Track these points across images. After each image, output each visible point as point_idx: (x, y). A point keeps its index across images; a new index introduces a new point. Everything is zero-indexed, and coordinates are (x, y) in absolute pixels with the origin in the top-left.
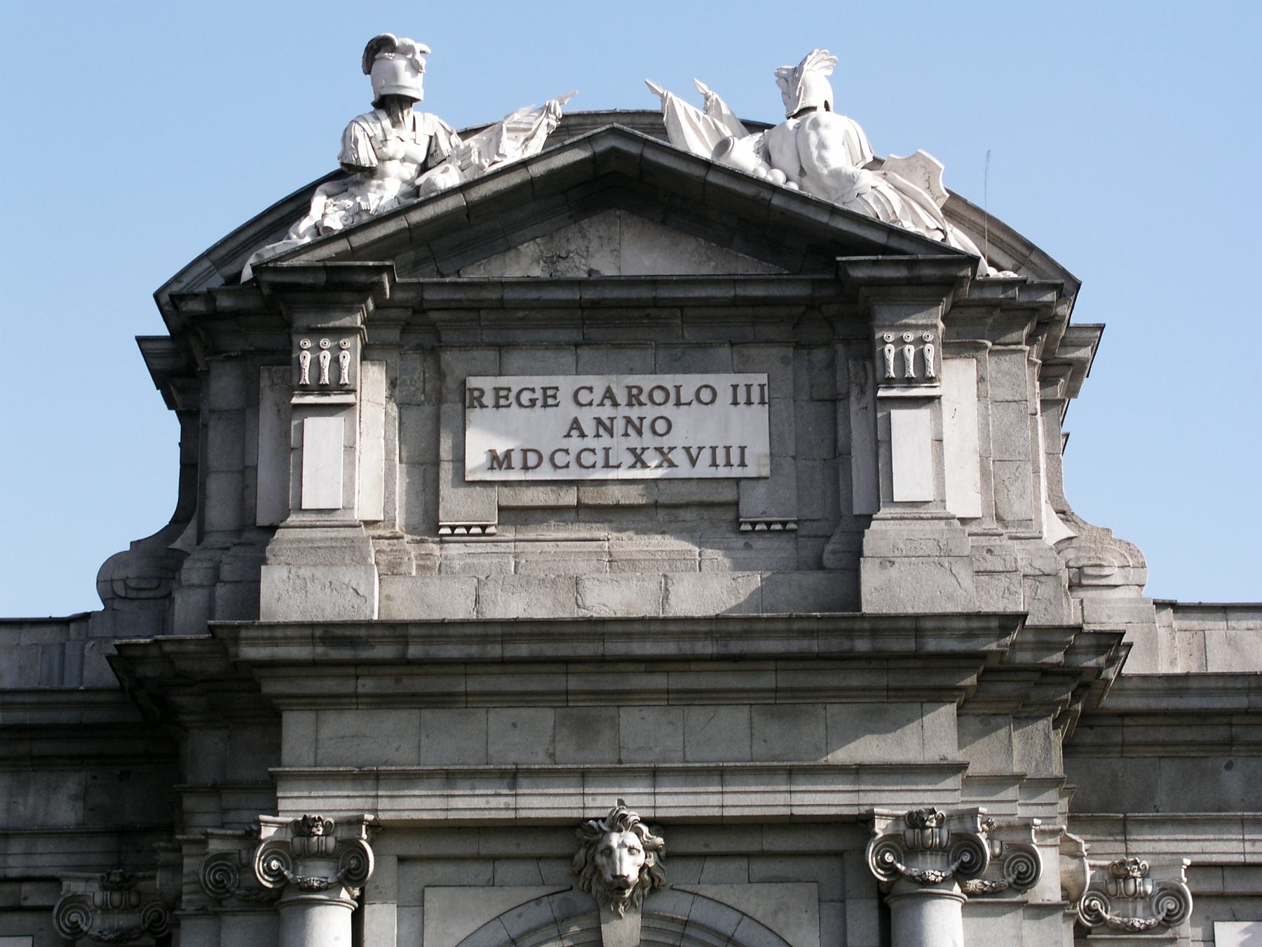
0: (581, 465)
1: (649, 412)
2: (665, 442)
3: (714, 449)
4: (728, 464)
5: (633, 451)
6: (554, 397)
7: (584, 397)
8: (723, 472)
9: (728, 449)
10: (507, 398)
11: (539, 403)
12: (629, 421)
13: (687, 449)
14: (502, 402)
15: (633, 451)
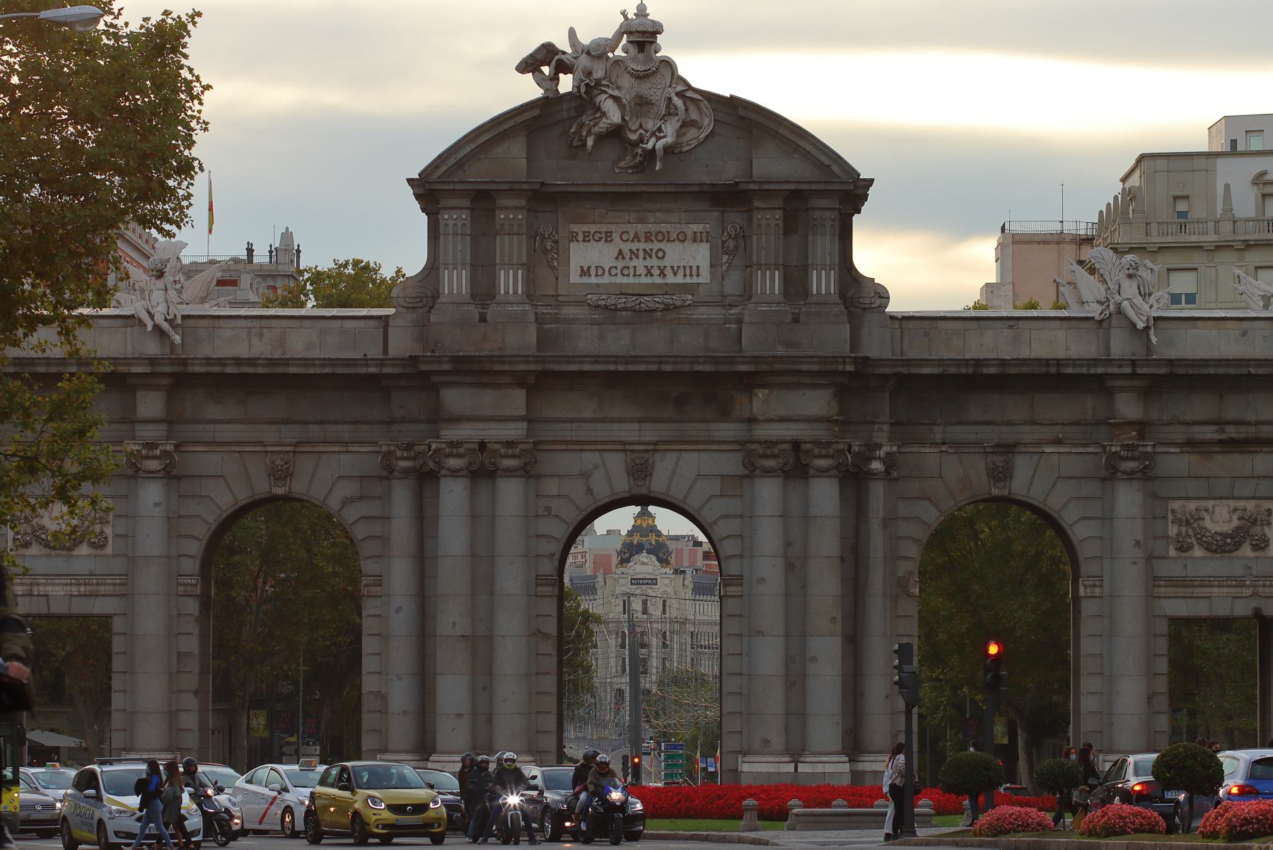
0: (623, 275)
1: (656, 246)
2: (661, 263)
3: (685, 267)
4: (691, 275)
5: (646, 267)
6: (610, 236)
7: (624, 238)
8: (688, 280)
9: (691, 267)
10: (588, 236)
11: (603, 240)
12: (645, 250)
13: (672, 267)
14: (587, 239)
15: (646, 267)
